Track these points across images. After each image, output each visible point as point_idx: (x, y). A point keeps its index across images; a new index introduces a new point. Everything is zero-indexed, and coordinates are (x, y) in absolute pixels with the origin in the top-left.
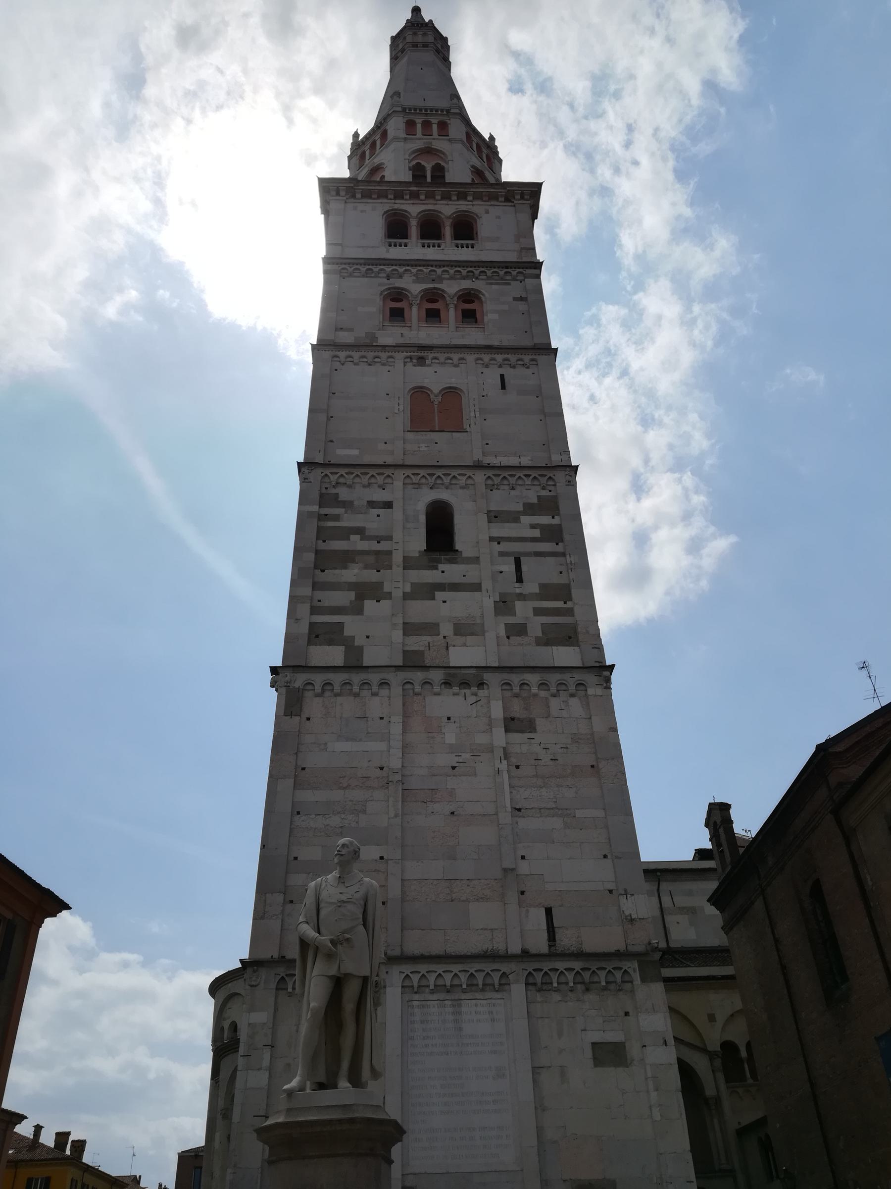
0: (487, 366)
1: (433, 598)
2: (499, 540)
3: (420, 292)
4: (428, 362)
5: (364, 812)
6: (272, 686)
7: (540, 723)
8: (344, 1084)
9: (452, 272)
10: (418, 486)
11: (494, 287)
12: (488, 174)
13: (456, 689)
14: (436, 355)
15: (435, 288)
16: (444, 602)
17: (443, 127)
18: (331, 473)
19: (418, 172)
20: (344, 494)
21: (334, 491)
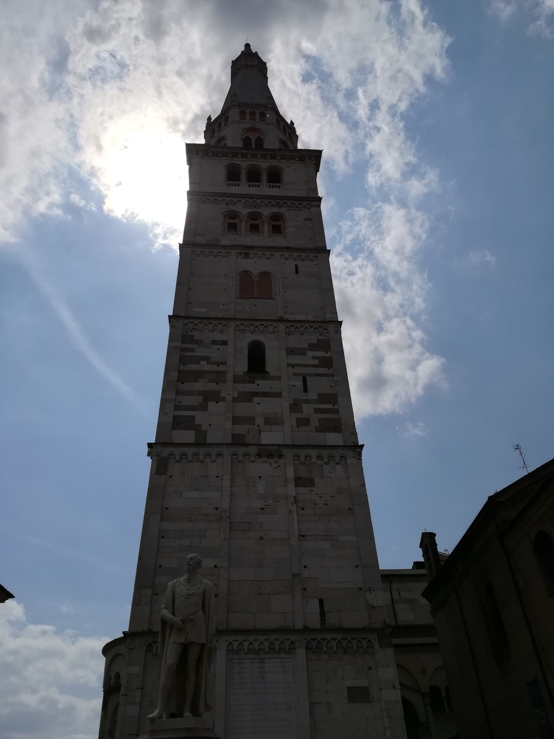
0: (287, 260)
1: (252, 402)
2: (293, 366)
4: (251, 256)
6: (148, 456)
8: (187, 714)
9: (266, 202)
10: (244, 331)
12: (289, 144)
13: (265, 459)
16: (258, 404)
19: (247, 142)
20: (197, 335)
21: (191, 334)
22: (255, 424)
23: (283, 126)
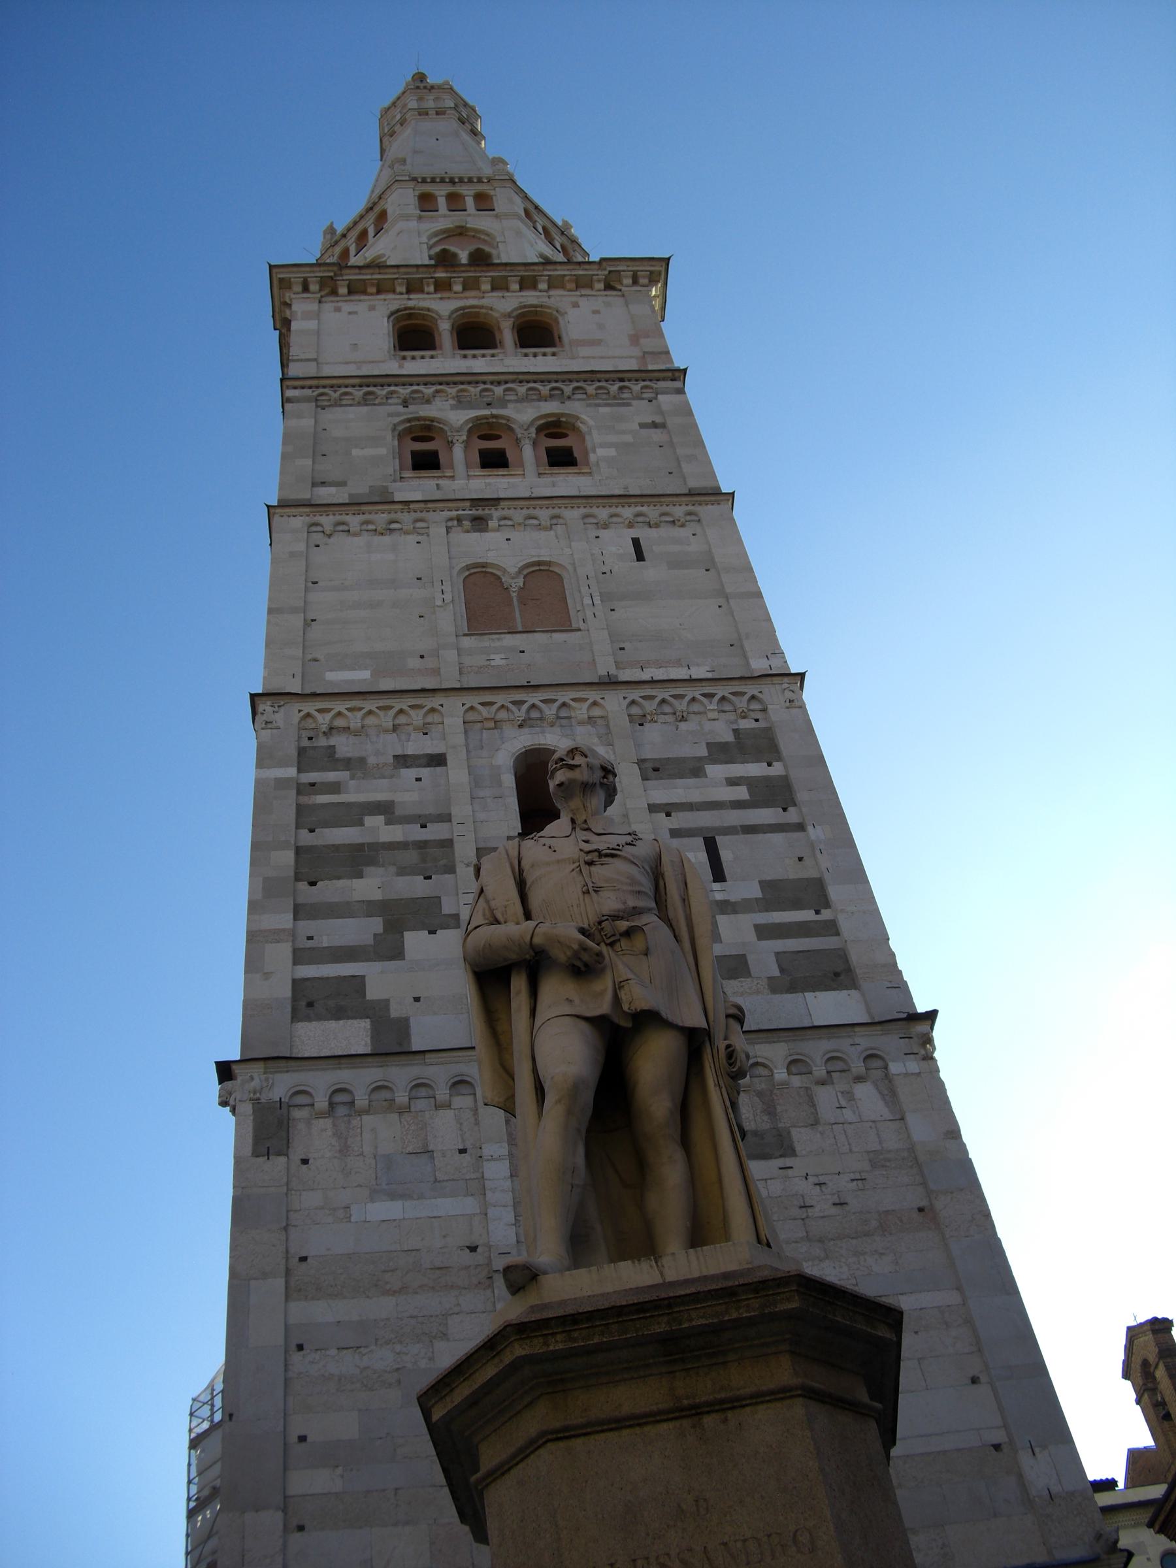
0: (606, 526)
2: (668, 810)
3: (467, 422)
4: (492, 524)
5: (444, 1336)
6: (223, 1103)
7: (801, 1137)
9: (522, 390)
11: (603, 410)
14: (506, 513)
15: (493, 416)
17: (484, 202)
18: (319, 711)
19: (445, 259)
20: (344, 746)
21: (322, 742)
23: (544, 228)
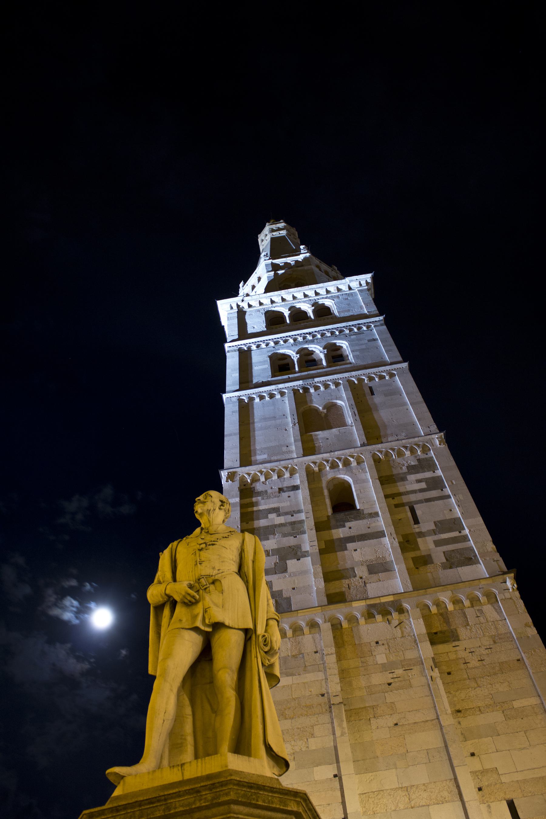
1: (346, 549)
5: (312, 735)
7: (463, 632)
11: (352, 337)
16: (355, 550)
20: (259, 487)
22: (355, 576)
